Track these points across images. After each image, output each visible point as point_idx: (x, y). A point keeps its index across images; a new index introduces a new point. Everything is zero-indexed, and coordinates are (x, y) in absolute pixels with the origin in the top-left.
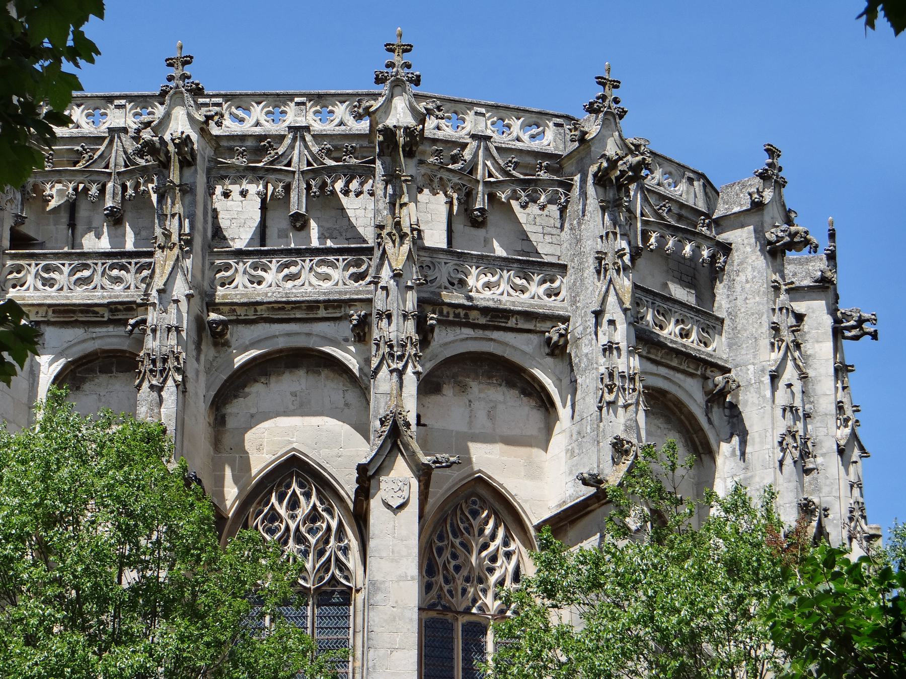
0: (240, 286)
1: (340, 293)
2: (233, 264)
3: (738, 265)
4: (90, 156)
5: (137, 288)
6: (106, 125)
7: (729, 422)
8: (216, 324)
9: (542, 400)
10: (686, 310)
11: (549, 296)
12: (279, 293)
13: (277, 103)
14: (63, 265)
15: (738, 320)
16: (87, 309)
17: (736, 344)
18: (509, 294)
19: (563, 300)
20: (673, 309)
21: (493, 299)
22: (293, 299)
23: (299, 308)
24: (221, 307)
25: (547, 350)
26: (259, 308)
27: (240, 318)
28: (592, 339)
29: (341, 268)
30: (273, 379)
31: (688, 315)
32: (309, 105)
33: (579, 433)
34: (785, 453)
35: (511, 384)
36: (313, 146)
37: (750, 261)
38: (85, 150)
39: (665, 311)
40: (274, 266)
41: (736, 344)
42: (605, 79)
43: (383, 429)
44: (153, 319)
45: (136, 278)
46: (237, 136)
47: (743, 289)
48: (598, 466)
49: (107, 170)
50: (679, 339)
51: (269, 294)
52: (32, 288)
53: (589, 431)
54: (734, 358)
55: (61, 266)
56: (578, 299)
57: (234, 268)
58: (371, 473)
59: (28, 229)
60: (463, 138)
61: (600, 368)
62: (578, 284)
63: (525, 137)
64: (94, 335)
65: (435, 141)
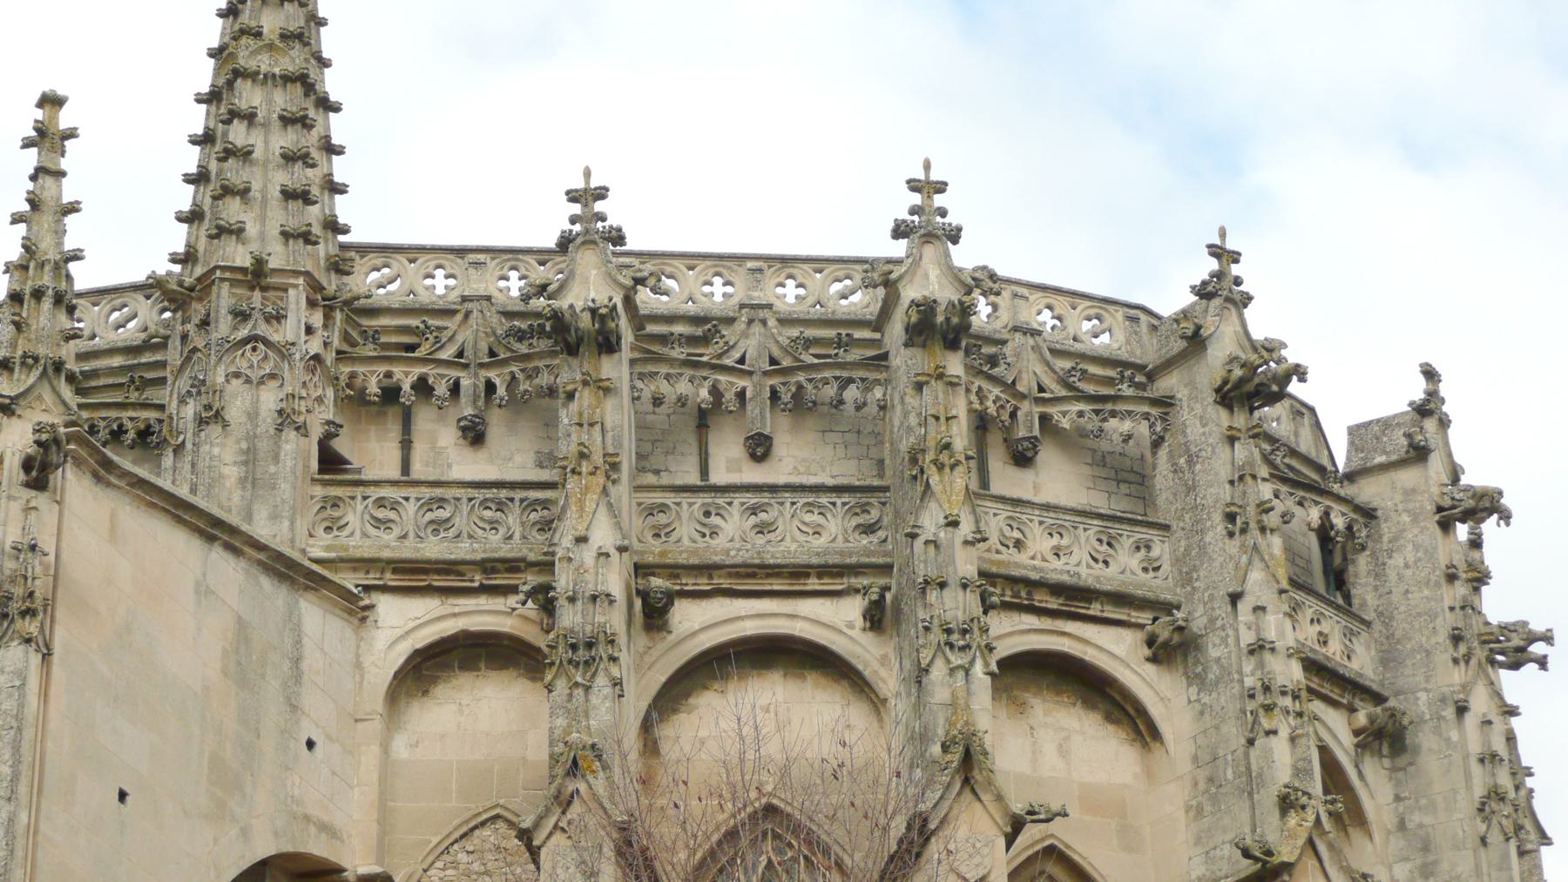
0: (686, 541)
1: (841, 553)
3: (1390, 542)
4: (436, 337)
5: (525, 537)
7: (1390, 779)
9: (1138, 732)
10: (1322, 605)
11: (1145, 570)
12: (747, 551)
13: (718, 269)
14: (407, 499)
15: (1395, 624)
16: (449, 567)
17: (1394, 660)
19: (1166, 579)
20: (1307, 602)
21: (1068, 572)
22: (771, 561)
23: (778, 575)
25: (1147, 652)
27: (686, 588)
28: (1227, 635)
29: (840, 516)
30: (732, 685)
31: (1326, 613)
32: (769, 273)
33: (1211, 780)
34: (1489, 826)
35: (1089, 705)
37: (1410, 536)
38: (427, 327)
39: (1297, 604)
40: (735, 510)
41: (1394, 660)
43: (949, 757)
44: (568, 583)
45: (523, 524)
47: (1400, 577)
48: (1254, 831)
49: (462, 361)
50: (1317, 647)
52: (358, 533)
53: (1230, 775)
54: (1393, 681)
55: (404, 502)
56: (1195, 576)
57: (674, 512)
58: (932, 826)
59: (341, 445)
60: (1000, 332)
61: (1246, 679)
62: (1193, 553)
64: (457, 610)
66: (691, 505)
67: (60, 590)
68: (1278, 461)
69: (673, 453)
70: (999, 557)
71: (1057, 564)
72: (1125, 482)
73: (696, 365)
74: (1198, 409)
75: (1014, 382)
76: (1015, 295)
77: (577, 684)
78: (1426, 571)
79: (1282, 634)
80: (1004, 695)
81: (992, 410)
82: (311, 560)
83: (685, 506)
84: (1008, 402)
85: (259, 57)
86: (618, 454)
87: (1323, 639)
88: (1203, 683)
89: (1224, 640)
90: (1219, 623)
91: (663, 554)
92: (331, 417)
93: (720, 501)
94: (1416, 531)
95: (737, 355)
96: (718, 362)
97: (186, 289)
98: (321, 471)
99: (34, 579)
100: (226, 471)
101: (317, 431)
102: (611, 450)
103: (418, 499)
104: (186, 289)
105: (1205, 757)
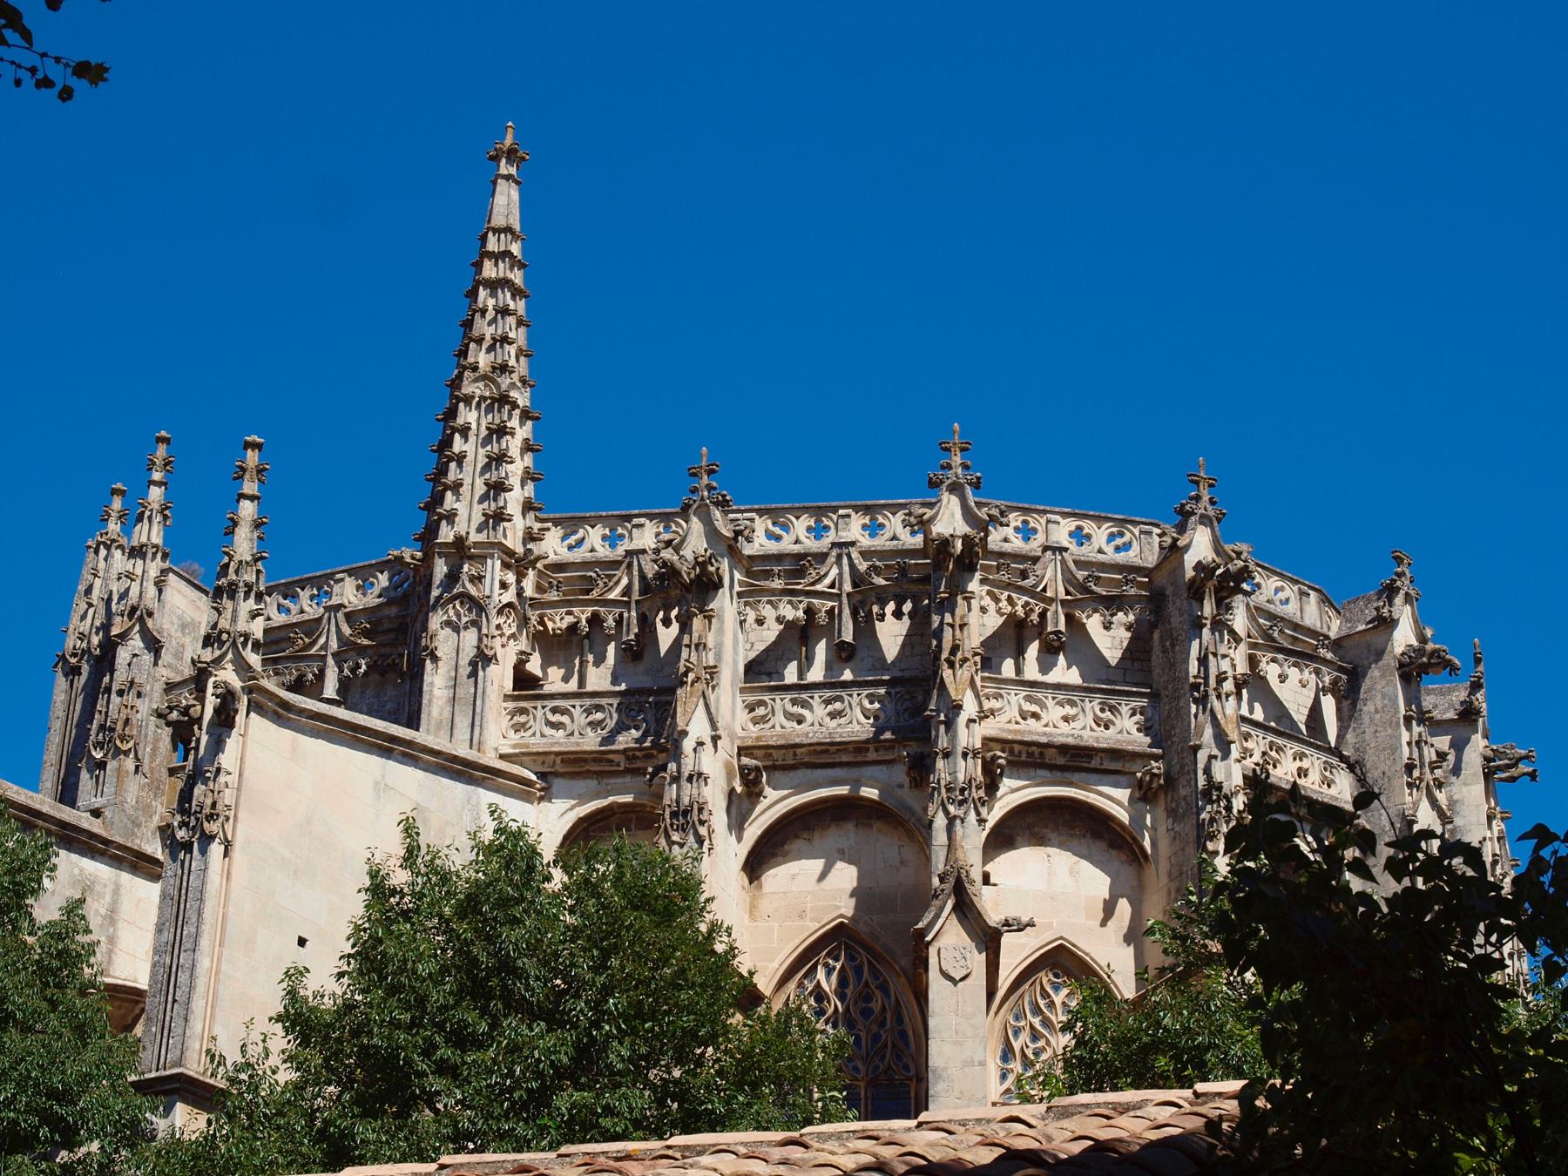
0: (778, 727)
2: (769, 702)
3: (1365, 693)
6: (624, 548)
8: (748, 769)
14: (574, 707)
18: (1092, 730)
21: (1073, 735)
22: (838, 740)
24: (755, 752)
26: (799, 751)
30: (817, 834)
36: (861, 564)
38: (599, 576)
42: (1195, 475)
46: (773, 555)
47: (1372, 720)
51: (811, 735)
52: (538, 734)
55: (571, 709)
58: (928, 938)
63: (1109, 549)
65: (1001, 555)
66: (782, 700)
67: (242, 801)
68: (1276, 634)
69: (781, 659)
70: (1017, 727)
71: (1065, 728)
72: (1139, 660)
73: (793, 593)
74: (1178, 604)
75: (1044, 590)
76: (1048, 521)
77: (674, 843)
78: (1390, 714)
79: (1229, 775)
80: (1027, 832)
81: (1020, 612)
82: (502, 757)
83: (778, 701)
84: (1037, 605)
85: (476, 384)
86: (715, 667)
87: (1302, 773)
88: (1176, 816)
89: (1189, 781)
90: (1186, 769)
91: (758, 739)
92: (523, 649)
93: (804, 696)
94: (1383, 683)
95: (827, 581)
96: (811, 588)
97: (418, 560)
98: (514, 690)
99: (219, 792)
100: (436, 692)
101: (513, 659)
102: (711, 664)
103: (581, 706)
104: (418, 560)
105: (1175, 873)
